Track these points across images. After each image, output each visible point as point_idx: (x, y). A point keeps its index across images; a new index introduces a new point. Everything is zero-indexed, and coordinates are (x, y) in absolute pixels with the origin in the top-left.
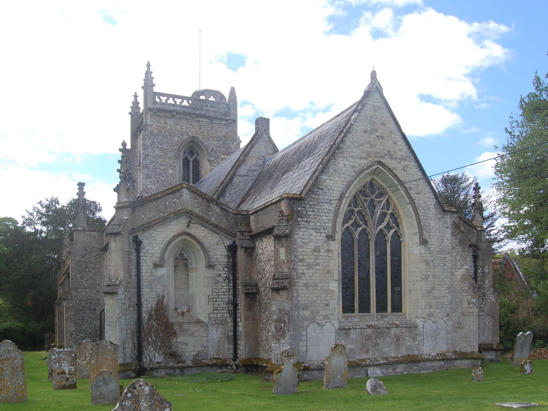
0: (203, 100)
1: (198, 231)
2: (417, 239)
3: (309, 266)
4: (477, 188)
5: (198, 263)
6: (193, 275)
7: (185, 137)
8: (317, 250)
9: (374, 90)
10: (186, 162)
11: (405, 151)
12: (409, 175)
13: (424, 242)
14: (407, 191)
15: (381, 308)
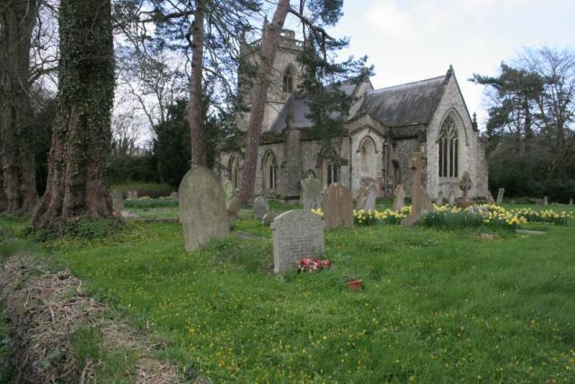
0: (282, 37)
1: (373, 135)
2: (465, 143)
3: (430, 155)
4: (475, 115)
5: (370, 149)
6: (368, 156)
7: (286, 64)
8: (432, 147)
9: (450, 73)
10: (285, 78)
11: (462, 103)
12: (463, 114)
13: (467, 145)
14: (462, 120)
15: (451, 175)
